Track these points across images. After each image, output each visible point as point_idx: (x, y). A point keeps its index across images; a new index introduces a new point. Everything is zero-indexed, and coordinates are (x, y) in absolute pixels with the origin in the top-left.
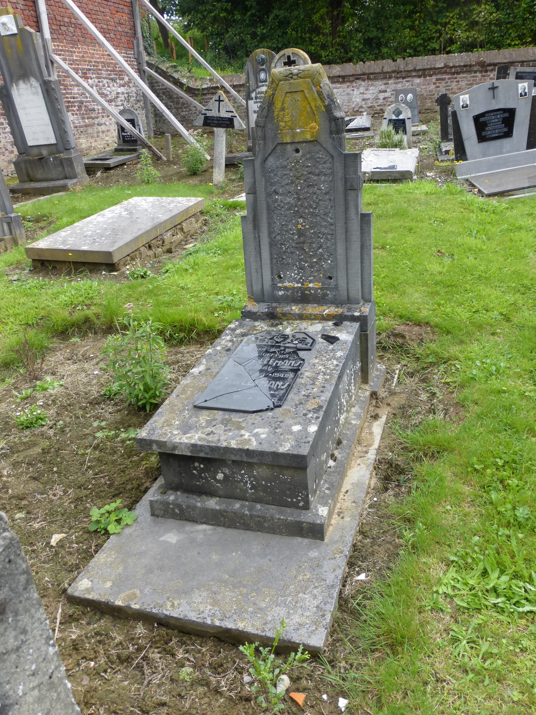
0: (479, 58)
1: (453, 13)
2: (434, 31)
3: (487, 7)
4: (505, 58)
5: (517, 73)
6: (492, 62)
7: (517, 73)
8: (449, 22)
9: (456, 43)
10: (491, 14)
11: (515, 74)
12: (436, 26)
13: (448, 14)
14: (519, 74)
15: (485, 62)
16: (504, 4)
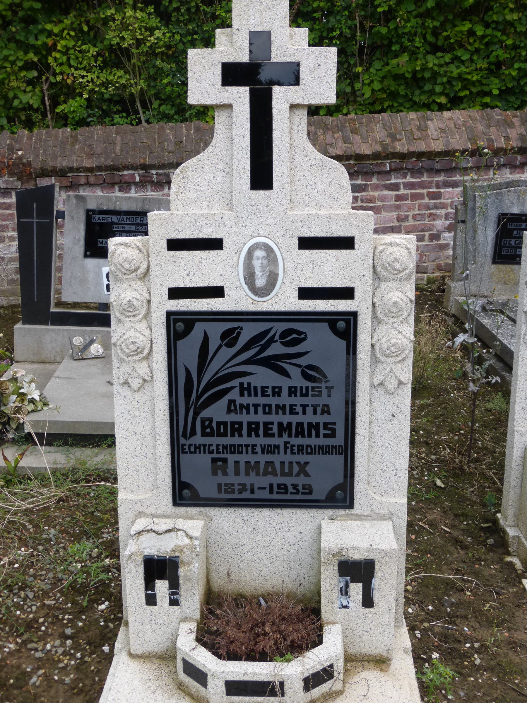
0: (11, 149)
1: (61, 26)
2: (20, 64)
3: (139, 14)
4: (90, 156)
5: (89, 214)
6: (50, 164)
7: (89, 214)
8: (55, 45)
9: (81, 95)
10: (151, 30)
11: (83, 218)
12: (26, 53)
13: (48, 27)
14: (97, 218)
15: (29, 164)
16: (177, 9)
